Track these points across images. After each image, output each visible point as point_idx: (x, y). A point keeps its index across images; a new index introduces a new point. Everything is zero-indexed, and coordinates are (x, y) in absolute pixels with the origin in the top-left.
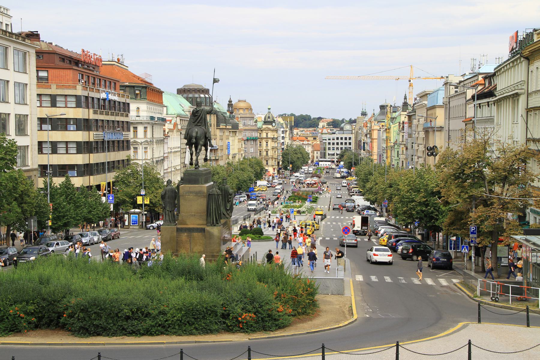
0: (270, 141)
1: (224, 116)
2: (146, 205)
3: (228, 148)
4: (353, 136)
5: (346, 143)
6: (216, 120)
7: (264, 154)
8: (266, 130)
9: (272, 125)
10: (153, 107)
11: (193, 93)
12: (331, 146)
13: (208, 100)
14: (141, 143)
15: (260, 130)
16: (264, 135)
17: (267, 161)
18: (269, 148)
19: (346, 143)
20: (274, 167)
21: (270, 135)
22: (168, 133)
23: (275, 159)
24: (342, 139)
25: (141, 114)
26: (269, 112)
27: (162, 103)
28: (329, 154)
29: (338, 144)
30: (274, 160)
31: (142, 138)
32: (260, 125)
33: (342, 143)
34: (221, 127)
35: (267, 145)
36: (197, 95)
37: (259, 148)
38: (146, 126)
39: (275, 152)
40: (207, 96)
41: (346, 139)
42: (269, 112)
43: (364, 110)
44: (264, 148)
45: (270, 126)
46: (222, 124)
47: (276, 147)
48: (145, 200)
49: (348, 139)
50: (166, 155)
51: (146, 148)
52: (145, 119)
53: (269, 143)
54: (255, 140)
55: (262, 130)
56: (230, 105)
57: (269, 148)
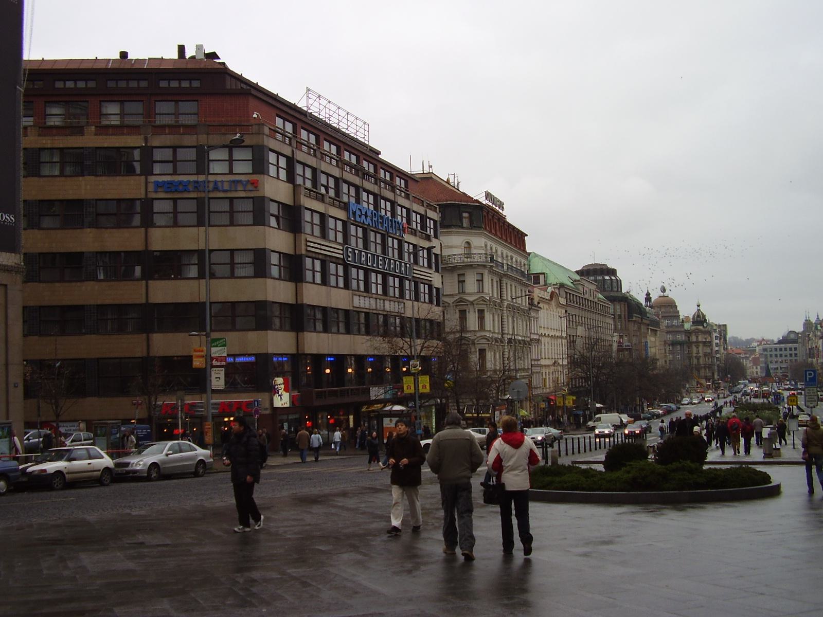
1: (639, 307)
2: (422, 396)
3: (646, 350)
5: (791, 355)
6: (626, 308)
7: (695, 361)
10: (500, 249)
11: (593, 275)
12: (774, 359)
13: (615, 284)
14: (472, 303)
15: (688, 333)
16: (694, 339)
17: (699, 371)
18: (701, 354)
21: (701, 338)
22: (539, 303)
24: (786, 349)
25: (474, 251)
26: (699, 310)
27: (524, 250)
30: (707, 370)
31: (474, 293)
32: (687, 326)
34: (634, 319)
35: (698, 352)
36: (599, 278)
38: (480, 271)
40: (613, 278)
41: (791, 349)
42: (699, 310)
43: (808, 318)
44: (694, 355)
45: (701, 327)
46: (635, 315)
47: (709, 353)
48: (421, 386)
49: (793, 349)
50: (532, 336)
51: (481, 312)
52: (477, 258)
53: (700, 348)
54: (681, 344)
56: (648, 298)
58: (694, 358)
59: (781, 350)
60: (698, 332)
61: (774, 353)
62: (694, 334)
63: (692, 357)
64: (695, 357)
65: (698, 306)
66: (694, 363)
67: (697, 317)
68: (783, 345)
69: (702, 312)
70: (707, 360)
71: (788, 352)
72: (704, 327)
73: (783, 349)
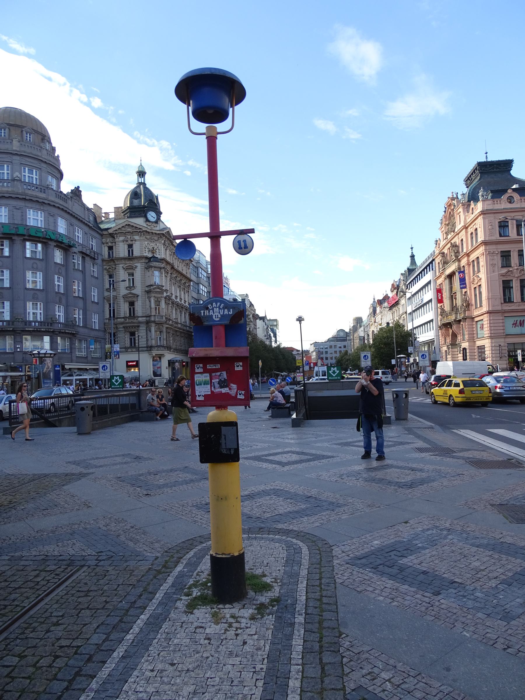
0: (139, 266)
7: (124, 309)
8: (125, 234)
9: (146, 217)
16: (121, 250)
17: (133, 334)
18: (138, 290)
23: (157, 324)
30: (153, 329)
44: (123, 291)
45: (139, 221)
55: (112, 235)
58: (122, 300)
59: (331, 347)
60: (132, 233)
62: (122, 238)
63: (115, 298)
64: (124, 297)
65: (141, 174)
69: (146, 189)
72: (147, 220)
73: (333, 347)
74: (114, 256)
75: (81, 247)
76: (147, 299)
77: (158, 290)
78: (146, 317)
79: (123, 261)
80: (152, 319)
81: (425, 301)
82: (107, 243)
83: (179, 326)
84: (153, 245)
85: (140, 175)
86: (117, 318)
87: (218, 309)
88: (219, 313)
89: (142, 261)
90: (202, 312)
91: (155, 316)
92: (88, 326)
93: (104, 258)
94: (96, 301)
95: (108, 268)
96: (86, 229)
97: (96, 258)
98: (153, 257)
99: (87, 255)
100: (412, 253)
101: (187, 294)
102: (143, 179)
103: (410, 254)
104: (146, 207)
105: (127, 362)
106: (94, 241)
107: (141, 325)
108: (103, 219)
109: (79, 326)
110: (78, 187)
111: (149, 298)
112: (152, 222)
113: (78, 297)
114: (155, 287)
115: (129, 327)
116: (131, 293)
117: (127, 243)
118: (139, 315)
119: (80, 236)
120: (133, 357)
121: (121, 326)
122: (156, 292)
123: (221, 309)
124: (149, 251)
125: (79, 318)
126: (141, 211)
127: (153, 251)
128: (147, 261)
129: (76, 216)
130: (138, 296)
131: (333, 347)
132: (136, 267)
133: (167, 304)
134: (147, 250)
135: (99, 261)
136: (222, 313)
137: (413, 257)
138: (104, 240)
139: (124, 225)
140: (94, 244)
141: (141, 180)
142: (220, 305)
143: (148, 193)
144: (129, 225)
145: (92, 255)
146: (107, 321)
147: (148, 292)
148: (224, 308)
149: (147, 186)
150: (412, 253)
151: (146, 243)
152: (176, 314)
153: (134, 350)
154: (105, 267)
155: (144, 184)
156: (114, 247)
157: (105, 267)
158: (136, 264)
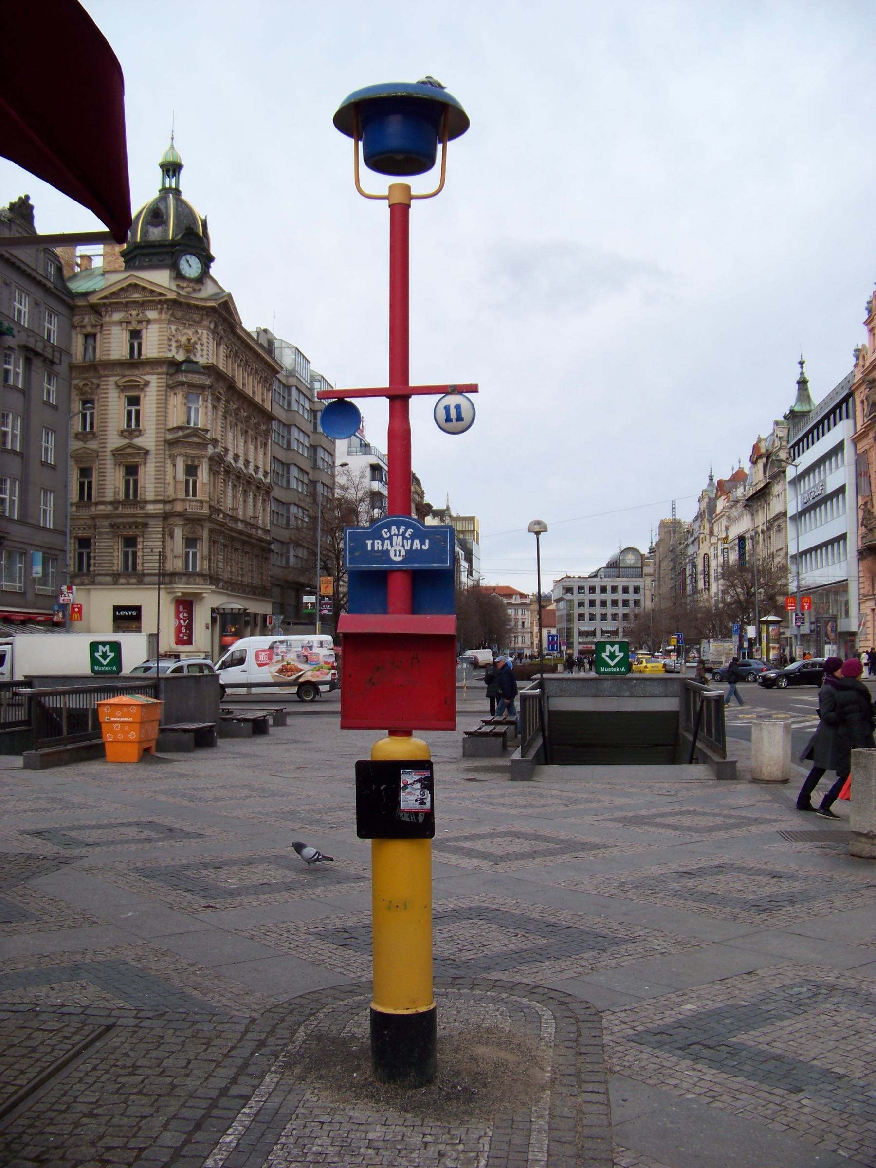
0: (155, 382)
4: (646, 583)
17: (130, 542)
19: (626, 603)
20: (181, 588)
24: (614, 589)
28: (579, 632)
29: (604, 604)
30: (178, 533)
33: (615, 603)
37: (75, 445)
39: (191, 470)
41: (626, 590)
44: (114, 441)
49: (631, 590)
55: (95, 309)
57: (148, 440)
58: (109, 462)
60: (143, 305)
61: (587, 597)
62: (117, 316)
63: (96, 455)
64: (117, 453)
66: (109, 497)
67: (147, 223)
68: (609, 579)
69: (181, 204)
70: (181, 475)
71: (620, 596)
72: (179, 276)
73: (609, 589)
74: (98, 356)
75: (23, 335)
76: (169, 461)
77: (195, 440)
78: (165, 502)
79: (118, 371)
80: (179, 507)
81: (830, 489)
82: (83, 327)
83: (241, 526)
84: (190, 332)
85: (168, 171)
86: (97, 504)
87: (400, 538)
88: (403, 546)
89: (160, 370)
90: (369, 542)
91: (183, 500)
92: (30, 521)
93: (74, 361)
94: (51, 461)
95: (81, 384)
96: (39, 294)
97: (57, 360)
98: (188, 361)
99: (37, 354)
100: (802, 373)
101: (261, 452)
102: (174, 180)
103: (797, 377)
104: (179, 245)
105: (117, 609)
106: (55, 320)
107: (152, 522)
108: (77, 269)
109: (10, 520)
110: (27, 197)
111: (173, 457)
112: (190, 280)
113: (13, 451)
114: (188, 431)
115: (124, 525)
116: (130, 446)
117: (130, 327)
118: (148, 498)
119: (25, 309)
120: (127, 597)
121: (106, 523)
122: (191, 444)
123: (407, 539)
124: (178, 347)
125: (12, 502)
126: (167, 253)
127: (190, 348)
128: (172, 371)
129: (18, 263)
130: (147, 452)
131: (609, 589)
132: (147, 383)
133: (213, 472)
134: (174, 344)
135: (62, 369)
136: (408, 547)
137: (802, 383)
138: (77, 319)
139: (124, 284)
140: (54, 328)
141: (171, 183)
142: (406, 530)
143: (185, 213)
144: (136, 286)
145: (48, 354)
146: (74, 509)
147: (171, 444)
148: (413, 537)
149: (184, 196)
150: (802, 373)
151: (173, 327)
152: (234, 497)
153: (133, 580)
154: (75, 382)
155: (177, 192)
156: (98, 337)
157: (75, 382)
158: (147, 378)
